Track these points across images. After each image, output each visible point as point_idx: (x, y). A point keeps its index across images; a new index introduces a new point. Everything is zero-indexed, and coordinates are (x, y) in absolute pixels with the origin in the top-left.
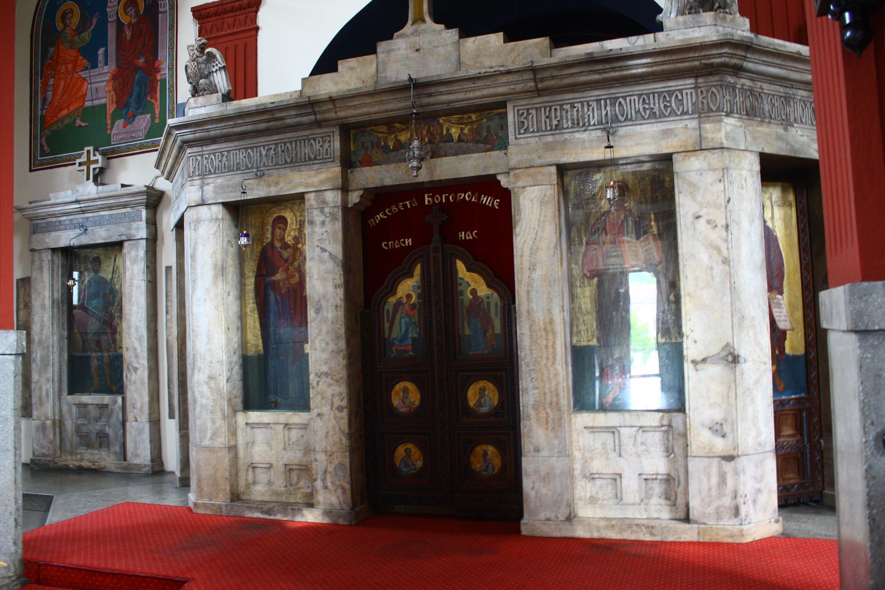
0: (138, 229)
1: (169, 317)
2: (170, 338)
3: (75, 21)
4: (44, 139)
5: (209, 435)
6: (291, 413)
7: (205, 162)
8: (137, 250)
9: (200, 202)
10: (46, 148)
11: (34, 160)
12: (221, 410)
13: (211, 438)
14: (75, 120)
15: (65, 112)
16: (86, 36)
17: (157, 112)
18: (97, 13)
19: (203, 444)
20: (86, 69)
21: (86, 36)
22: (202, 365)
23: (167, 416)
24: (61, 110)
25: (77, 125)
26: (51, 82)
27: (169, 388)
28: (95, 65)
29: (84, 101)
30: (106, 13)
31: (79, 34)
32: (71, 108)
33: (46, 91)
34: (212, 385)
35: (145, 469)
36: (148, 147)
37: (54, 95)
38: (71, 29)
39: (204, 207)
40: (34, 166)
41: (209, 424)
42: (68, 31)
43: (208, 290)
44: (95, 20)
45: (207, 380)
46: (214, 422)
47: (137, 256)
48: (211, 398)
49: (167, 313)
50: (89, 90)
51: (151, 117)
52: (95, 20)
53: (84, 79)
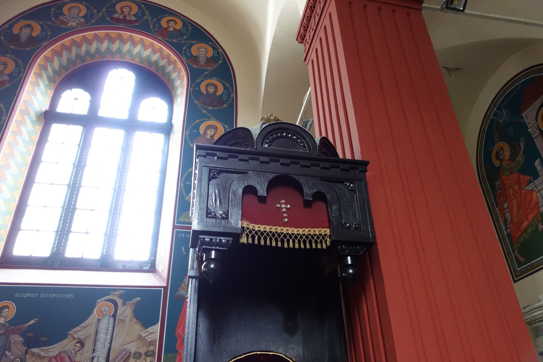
3: (507, 153)
4: (516, 252)
10: (520, 259)
11: (515, 272)
14: (537, 226)
15: (526, 223)
16: (520, 159)
18: (522, 138)
20: (530, 182)
21: (520, 159)
24: (522, 223)
25: (540, 229)
26: (506, 205)
28: (536, 175)
29: (538, 208)
30: (529, 133)
31: (514, 161)
32: (529, 218)
33: (504, 214)
37: (511, 214)
38: (506, 160)
40: (516, 277)
42: (504, 163)
44: (522, 144)
50: (540, 197)
52: (522, 144)
53: (532, 190)
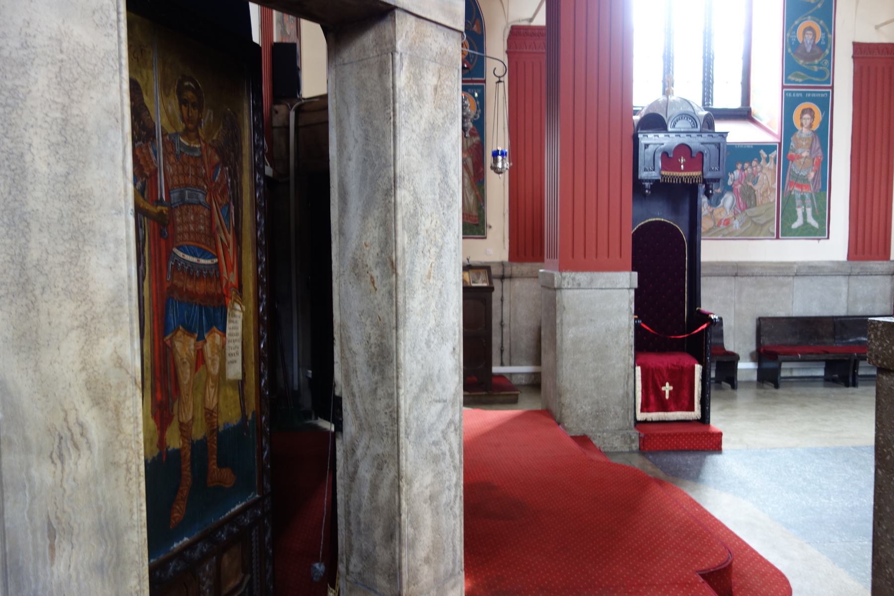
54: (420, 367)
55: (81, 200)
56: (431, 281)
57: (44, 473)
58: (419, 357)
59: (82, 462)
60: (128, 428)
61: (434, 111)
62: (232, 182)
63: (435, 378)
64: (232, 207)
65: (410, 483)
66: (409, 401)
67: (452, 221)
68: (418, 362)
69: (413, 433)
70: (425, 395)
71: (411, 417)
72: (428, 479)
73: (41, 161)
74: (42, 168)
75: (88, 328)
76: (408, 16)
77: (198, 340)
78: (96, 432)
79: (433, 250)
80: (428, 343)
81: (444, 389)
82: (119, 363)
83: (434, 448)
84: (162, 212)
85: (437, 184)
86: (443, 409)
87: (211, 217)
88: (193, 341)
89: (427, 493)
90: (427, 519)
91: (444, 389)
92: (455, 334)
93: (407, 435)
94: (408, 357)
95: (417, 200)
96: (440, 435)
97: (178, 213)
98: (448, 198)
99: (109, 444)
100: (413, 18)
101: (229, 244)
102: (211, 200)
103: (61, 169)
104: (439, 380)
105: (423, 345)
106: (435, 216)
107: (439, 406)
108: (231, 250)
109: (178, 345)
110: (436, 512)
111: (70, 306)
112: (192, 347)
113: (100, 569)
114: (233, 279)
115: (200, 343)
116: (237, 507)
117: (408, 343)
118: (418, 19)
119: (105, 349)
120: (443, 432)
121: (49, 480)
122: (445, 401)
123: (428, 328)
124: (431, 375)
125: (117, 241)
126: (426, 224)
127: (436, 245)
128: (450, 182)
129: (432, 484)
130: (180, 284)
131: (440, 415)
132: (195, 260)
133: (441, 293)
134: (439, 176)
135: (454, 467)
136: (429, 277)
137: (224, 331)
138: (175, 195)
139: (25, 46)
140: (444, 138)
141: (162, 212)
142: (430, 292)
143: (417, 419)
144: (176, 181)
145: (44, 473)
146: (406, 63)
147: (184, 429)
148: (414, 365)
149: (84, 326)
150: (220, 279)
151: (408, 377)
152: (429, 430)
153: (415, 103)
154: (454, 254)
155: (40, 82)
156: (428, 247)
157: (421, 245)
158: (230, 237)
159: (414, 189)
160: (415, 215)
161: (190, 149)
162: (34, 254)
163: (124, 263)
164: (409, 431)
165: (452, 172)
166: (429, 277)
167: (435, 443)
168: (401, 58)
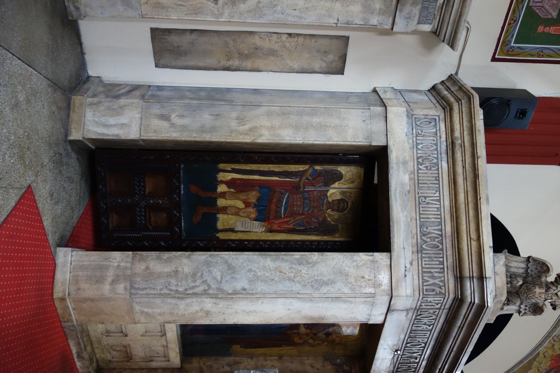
0: (408, 18)
1: (284, 38)
2: (257, 37)
5: (146, 310)
6: (178, 351)
7: (432, 311)
8: (381, 12)
9: (392, 308)
12: (174, 320)
13: (142, 312)
17: (552, 30)
19: (134, 304)
22: (221, 306)
23: (155, 25)
27: (192, 31)
34: (200, 314)
35: (72, 8)
36: (514, 11)
39: (386, 310)
41: (158, 311)
43: (299, 312)
45: (205, 309)
46: (160, 314)
47: (372, 13)
48: (186, 313)
49: (290, 35)
51: (552, 19)
54: (240, 264)
55: (306, 128)
56: (278, 273)
57: (234, 115)
58: (245, 264)
59: (235, 124)
60: (241, 137)
61: (354, 276)
62: (312, 228)
63: (233, 275)
64: (302, 228)
65: (188, 257)
66: (226, 256)
67: (306, 288)
68: (242, 263)
69: (211, 259)
70: (226, 268)
71: (219, 258)
72: (187, 270)
73: (315, 120)
74: (314, 120)
75: (272, 128)
76: (389, 260)
77: (255, 204)
78: (242, 128)
79: (292, 275)
80: (250, 270)
81: (226, 282)
82: (261, 136)
83: (199, 274)
84: (301, 188)
85: (322, 278)
86: (217, 281)
87: (299, 214)
88: (254, 201)
89: (180, 269)
90: (168, 269)
91: (226, 282)
92: (252, 290)
93: (210, 256)
94: (246, 256)
95: (315, 264)
96: (205, 279)
97: (300, 196)
98: (316, 286)
99: (238, 131)
100: (389, 263)
101: (288, 225)
102: (305, 215)
103: (314, 124)
104: (232, 278)
105: (250, 267)
106: (308, 276)
107: (219, 278)
108: (286, 226)
109: (254, 193)
110: (169, 275)
111: (278, 124)
112: (252, 201)
113: (203, 126)
114: (275, 227)
115: (253, 205)
116: (183, 224)
117: (251, 257)
118: (389, 267)
119: (265, 132)
120: (206, 280)
121: (232, 116)
122: (221, 283)
123: (257, 271)
124: (234, 272)
125: (295, 137)
126: (304, 270)
127: (295, 277)
128: (323, 287)
129: (183, 272)
130: (276, 195)
131: (215, 278)
132: (284, 204)
133: (273, 280)
134: (325, 279)
135: (186, 290)
136: (281, 272)
137: (256, 220)
138: (306, 195)
139: (344, 118)
140: (343, 282)
141: (301, 188)
142: (273, 272)
143: (217, 262)
144: (312, 196)
145: (234, 115)
146: (370, 258)
147: (223, 195)
148: (241, 261)
149: (272, 127)
150: (276, 218)
151: (237, 256)
152: (209, 271)
153: (355, 263)
154: (290, 290)
155: (336, 121)
156: (293, 271)
157: (294, 266)
158: (291, 226)
159: (318, 262)
160: (308, 263)
161: (323, 204)
162: (292, 117)
163: (289, 139)
164: (212, 257)
165: (328, 289)
166: (281, 272)
167: (202, 275)
168: (371, 255)
